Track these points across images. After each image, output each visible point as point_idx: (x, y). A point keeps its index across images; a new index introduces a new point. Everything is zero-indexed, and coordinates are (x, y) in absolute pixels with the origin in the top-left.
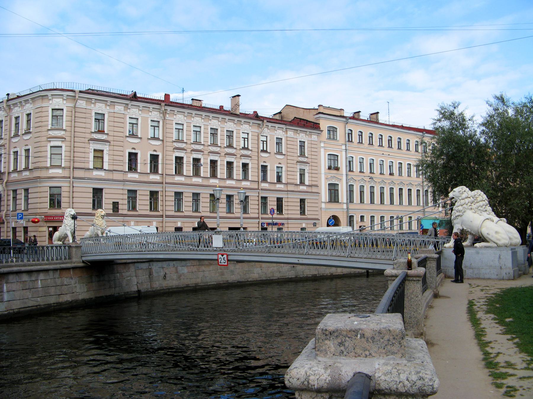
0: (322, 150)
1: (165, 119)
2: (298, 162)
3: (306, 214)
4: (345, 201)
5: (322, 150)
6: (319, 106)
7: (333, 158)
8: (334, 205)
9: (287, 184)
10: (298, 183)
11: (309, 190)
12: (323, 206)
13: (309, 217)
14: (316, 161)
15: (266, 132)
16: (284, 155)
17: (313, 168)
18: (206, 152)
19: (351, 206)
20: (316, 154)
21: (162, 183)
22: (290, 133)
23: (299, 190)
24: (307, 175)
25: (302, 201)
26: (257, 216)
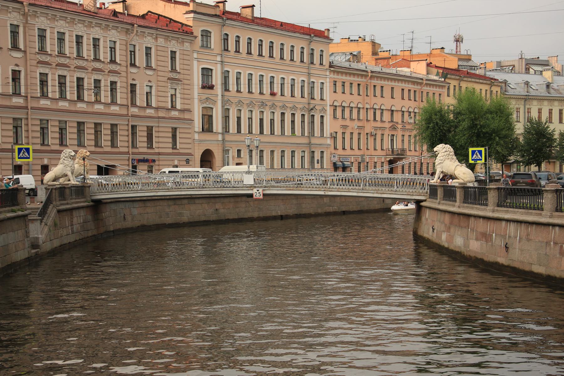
0: (195, 63)
1: (27, 23)
2: (169, 79)
3: (178, 147)
4: (220, 130)
5: (195, 63)
7: (207, 73)
8: (207, 136)
9: (157, 109)
10: (170, 107)
12: (196, 136)
13: (182, 151)
14: (188, 77)
15: (136, 40)
16: (155, 70)
17: (186, 87)
18: (72, 67)
19: (228, 138)
21: (26, 108)
22: (161, 41)
23: (170, 116)
24: (178, 95)
25: (174, 130)
26: (126, 150)
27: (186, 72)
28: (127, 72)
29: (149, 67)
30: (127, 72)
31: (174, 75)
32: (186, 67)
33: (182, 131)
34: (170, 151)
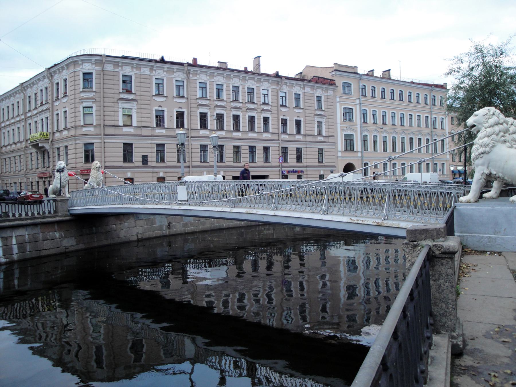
4: (360, 150)
5: (338, 105)
9: (305, 135)
11: (326, 140)
13: (327, 164)
14: (332, 114)
16: (303, 109)
28: (278, 111)
29: (298, 106)
30: (278, 111)
34: (317, 164)
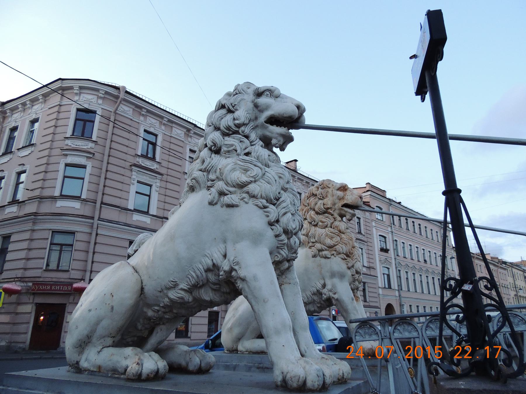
0: (374, 230)
3: (368, 300)
4: (397, 288)
5: (374, 230)
6: (367, 184)
8: (388, 292)
12: (380, 291)
13: (371, 304)
20: (369, 234)
27: (369, 236)
31: (360, 237)
32: (368, 232)
33: (370, 285)
